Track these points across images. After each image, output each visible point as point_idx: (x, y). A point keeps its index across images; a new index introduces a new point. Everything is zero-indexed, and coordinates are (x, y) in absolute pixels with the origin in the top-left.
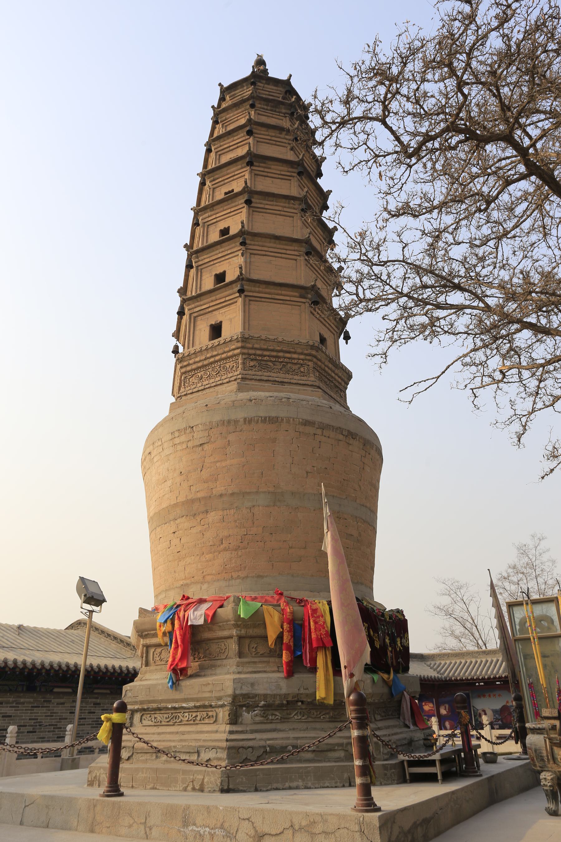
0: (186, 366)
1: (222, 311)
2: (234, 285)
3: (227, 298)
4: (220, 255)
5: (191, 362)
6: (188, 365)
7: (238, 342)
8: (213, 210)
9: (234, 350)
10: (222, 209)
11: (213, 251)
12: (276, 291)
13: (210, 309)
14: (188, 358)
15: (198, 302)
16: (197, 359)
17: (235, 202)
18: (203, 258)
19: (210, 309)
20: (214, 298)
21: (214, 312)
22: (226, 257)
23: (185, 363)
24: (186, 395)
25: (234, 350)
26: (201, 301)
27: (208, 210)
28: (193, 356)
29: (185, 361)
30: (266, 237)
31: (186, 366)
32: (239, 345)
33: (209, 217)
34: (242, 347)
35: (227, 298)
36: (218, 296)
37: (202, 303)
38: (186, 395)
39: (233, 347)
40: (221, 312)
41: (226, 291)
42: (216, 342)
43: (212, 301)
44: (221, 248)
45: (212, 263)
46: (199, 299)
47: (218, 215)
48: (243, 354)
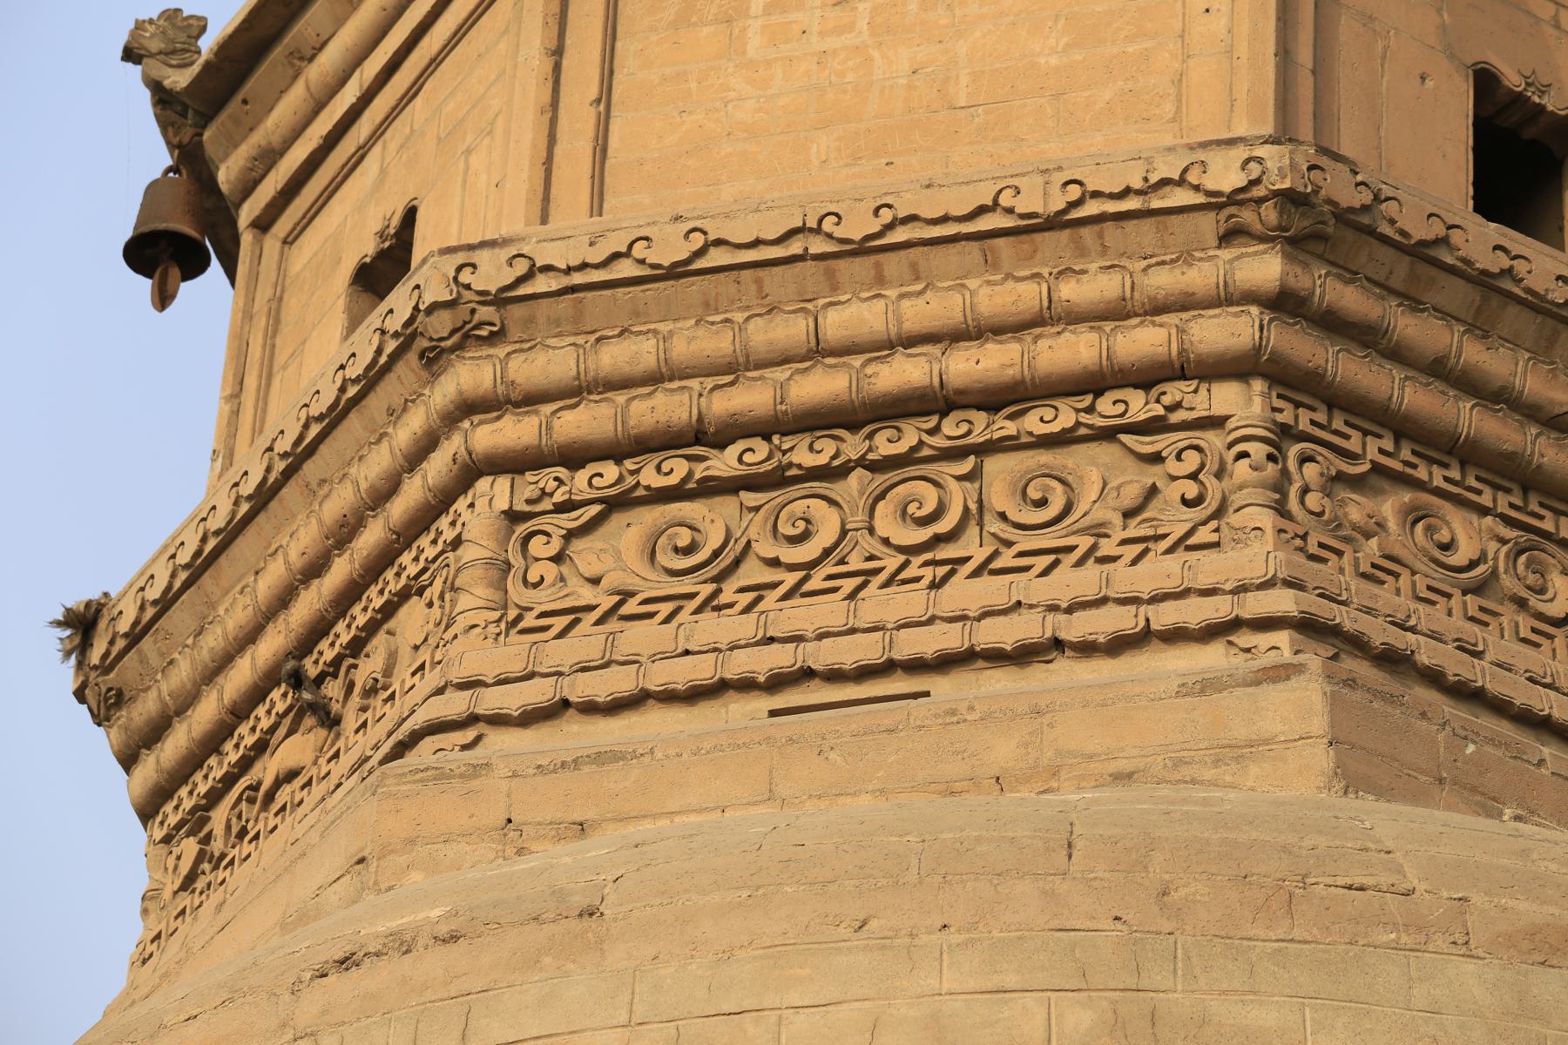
0: (1332, 324)
28: (1455, 294)
31: (1332, 324)
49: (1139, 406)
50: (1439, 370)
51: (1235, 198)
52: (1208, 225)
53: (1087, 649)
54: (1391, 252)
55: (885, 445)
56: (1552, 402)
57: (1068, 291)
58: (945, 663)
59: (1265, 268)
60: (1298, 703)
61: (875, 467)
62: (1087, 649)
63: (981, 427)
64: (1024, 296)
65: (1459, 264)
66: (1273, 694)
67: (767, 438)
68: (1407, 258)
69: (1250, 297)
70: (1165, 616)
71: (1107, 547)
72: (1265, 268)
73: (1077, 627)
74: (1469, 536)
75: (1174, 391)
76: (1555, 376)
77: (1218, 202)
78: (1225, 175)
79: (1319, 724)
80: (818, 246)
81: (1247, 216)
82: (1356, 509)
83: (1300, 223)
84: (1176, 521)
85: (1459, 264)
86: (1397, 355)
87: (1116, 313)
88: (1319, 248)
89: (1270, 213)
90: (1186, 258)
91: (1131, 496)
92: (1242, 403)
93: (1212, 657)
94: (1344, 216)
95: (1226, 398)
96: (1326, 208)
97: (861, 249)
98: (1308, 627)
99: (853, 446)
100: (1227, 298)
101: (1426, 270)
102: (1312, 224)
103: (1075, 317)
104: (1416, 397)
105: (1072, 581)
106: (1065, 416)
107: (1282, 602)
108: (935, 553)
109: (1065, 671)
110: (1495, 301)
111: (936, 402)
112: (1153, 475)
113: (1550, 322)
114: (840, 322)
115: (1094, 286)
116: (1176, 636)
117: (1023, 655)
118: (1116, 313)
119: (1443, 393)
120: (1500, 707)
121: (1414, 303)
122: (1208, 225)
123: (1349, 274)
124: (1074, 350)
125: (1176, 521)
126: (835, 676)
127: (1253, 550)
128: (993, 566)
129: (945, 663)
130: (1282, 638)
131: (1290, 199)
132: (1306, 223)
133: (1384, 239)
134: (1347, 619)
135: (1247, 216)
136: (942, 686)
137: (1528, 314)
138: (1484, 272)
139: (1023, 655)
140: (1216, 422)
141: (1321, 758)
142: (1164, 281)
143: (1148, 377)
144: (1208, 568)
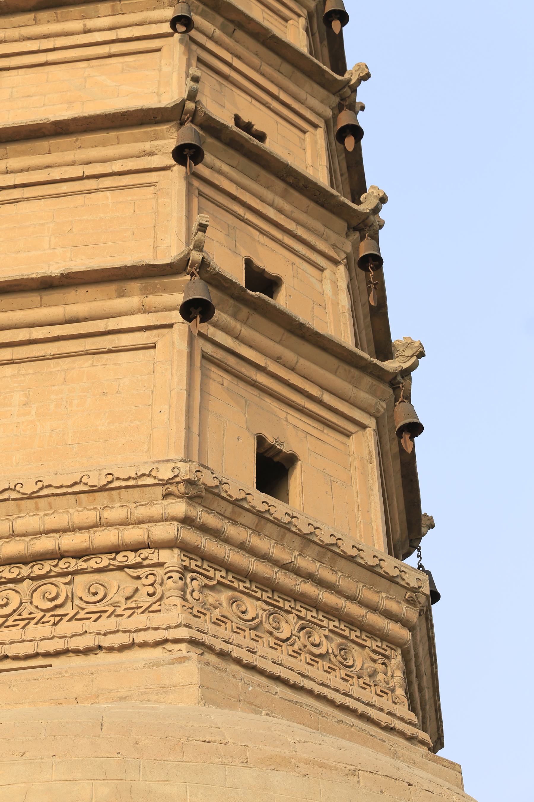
0: (204, 529)
1: (294, 418)
2: (368, 381)
3: (327, 398)
4: (271, 213)
8: (231, 35)
11: (255, 179)
13: (261, 378)
14: (229, 509)
15: (234, 316)
16: (256, 541)
18: (218, 164)
19: (261, 378)
20: (289, 356)
21: (268, 401)
26: (244, 322)
31: (204, 529)
33: (211, 38)
35: (327, 398)
36: (304, 364)
37: (246, 332)
41: (335, 373)
43: (278, 360)
44: (284, 196)
45: (240, 210)
46: (245, 311)
47: (237, 63)
49: (132, 558)
50: (242, 547)
51: (169, 482)
52: (159, 491)
53: (111, 649)
54: (226, 502)
55: (37, 571)
56: (283, 559)
57: (108, 515)
58: (58, 654)
59: (180, 508)
60: (187, 671)
61: (33, 579)
62: (111, 649)
63: (73, 564)
64: (91, 516)
65: (250, 508)
66: (179, 668)
68: (231, 505)
69: (174, 519)
70: (140, 638)
71: (119, 611)
72: (180, 508)
73: (106, 642)
74: (253, 608)
75: (145, 553)
76: (284, 550)
77: (163, 483)
78: (166, 473)
79: (196, 679)
80: (14, 495)
81: (173, 488)
82: (211, 597)
83: (193, 492)
84: (144, 601)
85: (250, 508)
86: (227, 541)
87: (125, 523)
88: (200, 501)
89: (182, 488)
90: (150, 503)
91: (129, 592)
92: (171, 558)
93: (157, 653)
94: (208, 489)
95: (164, 556)
96: (202, 486)
97: (30, 497)
98: (193, 642)
99: (25, 570)
100: (165, 519)
101: (238, 510)
102: (198, 493)
103: (109, 525)
104: (235, 557)
105: (106, 624)
106: (105, 561)
107: (183, 633)
108: (55, 611)
109: (102, 657)
110: (263, 521)
111: (58, 555)
112: (137, 584)
113: (283, 530)
114: (21, 525)
115: (116, 513)
116: (144, 645)
117: (87, 651)
118: (125, 523)
119: (244, 555)
120: (262, 672)
121: (234, 522)
122: (159, 491)
123: (211, 511)
124: (107, 537)
125: (144, 601)
126: (16, 658)
127: (173, 613)
128: (77, 617)
129: (58, 654)
130: (183, 646)
131: (190, 483)
132: (195, 492)
133: (223, 498)
134: (207, 640)
135: (173, 488)
136: (55, 662)
137: (275, 527)
138: (259, 511)
139: (87, 651)
140: (160, 565)
141: (196, 692)
142: (142, 512)
143: (135, 548)
144: (156, 620)
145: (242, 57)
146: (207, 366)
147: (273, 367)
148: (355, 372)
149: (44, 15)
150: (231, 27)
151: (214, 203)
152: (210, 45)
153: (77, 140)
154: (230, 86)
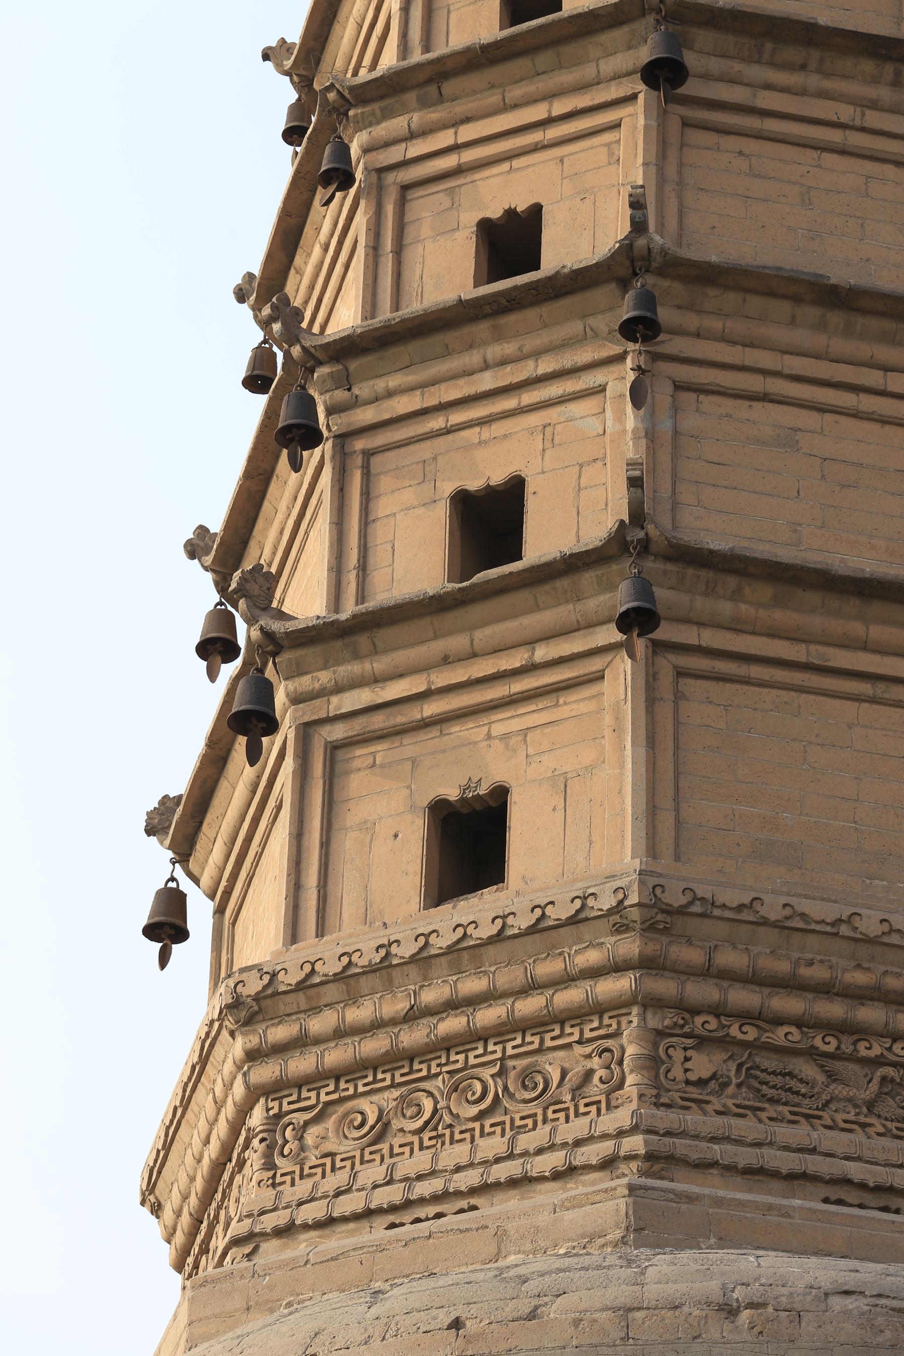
0: (281, 1049)
1: (505, 723)
2: (588, 578)
3: (542, 653)
4: (487, 381)
5: (318, 1024)
6: (301, 1042)
7: (621, 929)
8: (441, 99)
9: (594, 973)
10: (493, 99)
11: (448, 352)
12: (836, 626)
13: (431, 709)
14: (301, 999)
15: (357, 656)
17: (578, 63)
18: (380, 385)
19: (431, 709)
20: (457, 643)
21: (456, 729)
22: (529, 397)
23: (279, 1033)
24: (286, 1231)
25: (594, 973)
26: (375, 651)
27: (411, 97)
28: (332, 992)
29: (281, 1019)
30: (772, 294)
31: (281, 1049)
32: (630, 946)
33: (412, 136)
34: (647, 964)
35: (542, 653)
36: (484, 636)
37: (380, 664)
38: (286, 1231)
39: (592, 957)
40: (498, 729)
41: (537, 608)
42: (479, 910)
43: (446, 661)
45: (437, 423)
46: (363, 641)
47: (467, 133)
48: (650, 1003)
54: (291, 995)
56: (397, 1012)
65: (324, 978)
67: (717, 1016)
68: (301, 993)
76: (396, 997)
85: (324, 978)
88: (260, 1017)
96: (249, 1000)
101: (311, 992)
110: (352, 982)
113: (383, 972)
119: (345, 1044)
132: (244, 1013)
133: (285, 993)
137: (371, 977)
138: (335, 975)
145: (469, 115)
146: (347, 756)
147: (441, 679)
148: (562, 583)
149: (298, 260)
150: (432, 89)
151: (399, 447)
152: (417, 149)
153: (277, 477)
154: (478, 176)
